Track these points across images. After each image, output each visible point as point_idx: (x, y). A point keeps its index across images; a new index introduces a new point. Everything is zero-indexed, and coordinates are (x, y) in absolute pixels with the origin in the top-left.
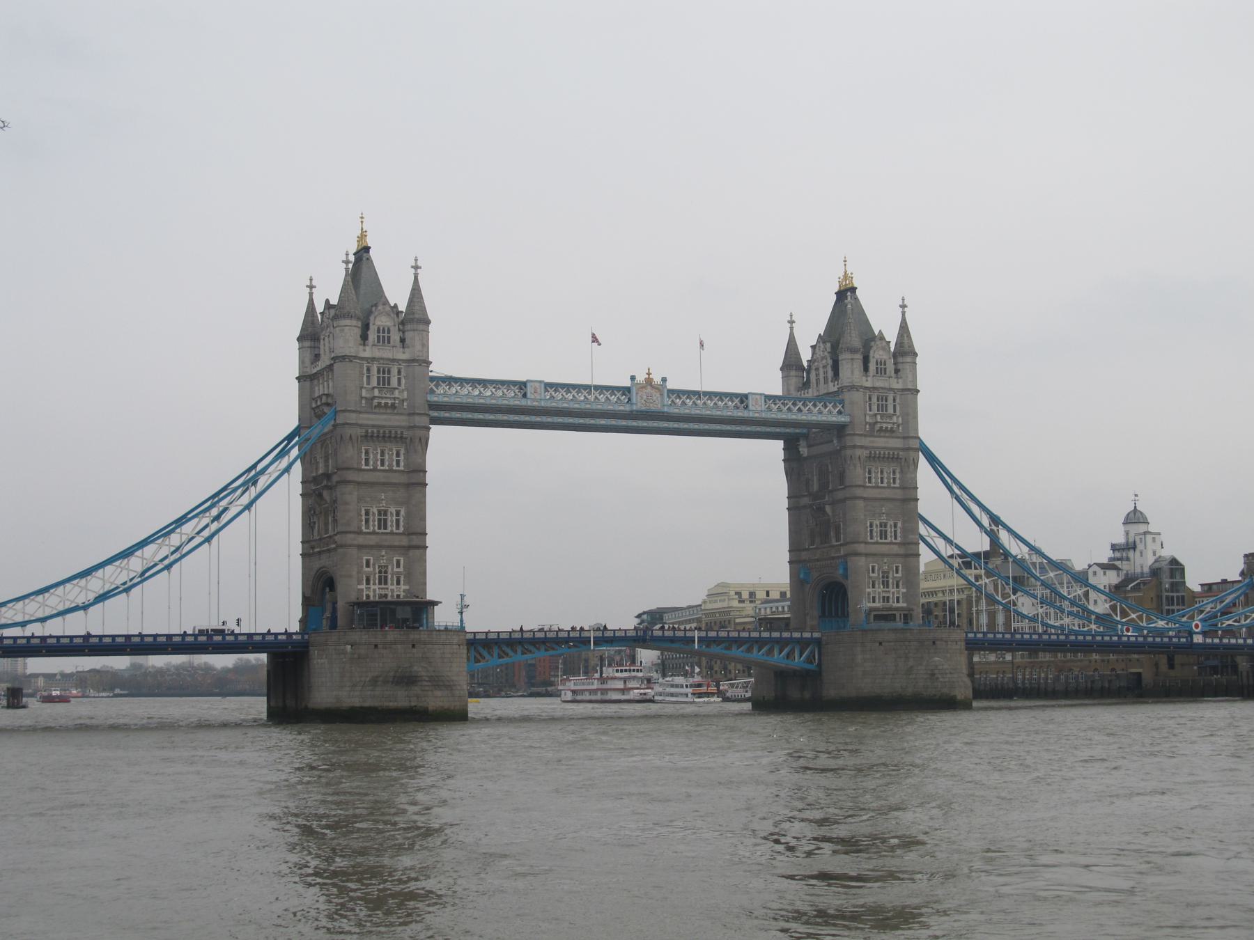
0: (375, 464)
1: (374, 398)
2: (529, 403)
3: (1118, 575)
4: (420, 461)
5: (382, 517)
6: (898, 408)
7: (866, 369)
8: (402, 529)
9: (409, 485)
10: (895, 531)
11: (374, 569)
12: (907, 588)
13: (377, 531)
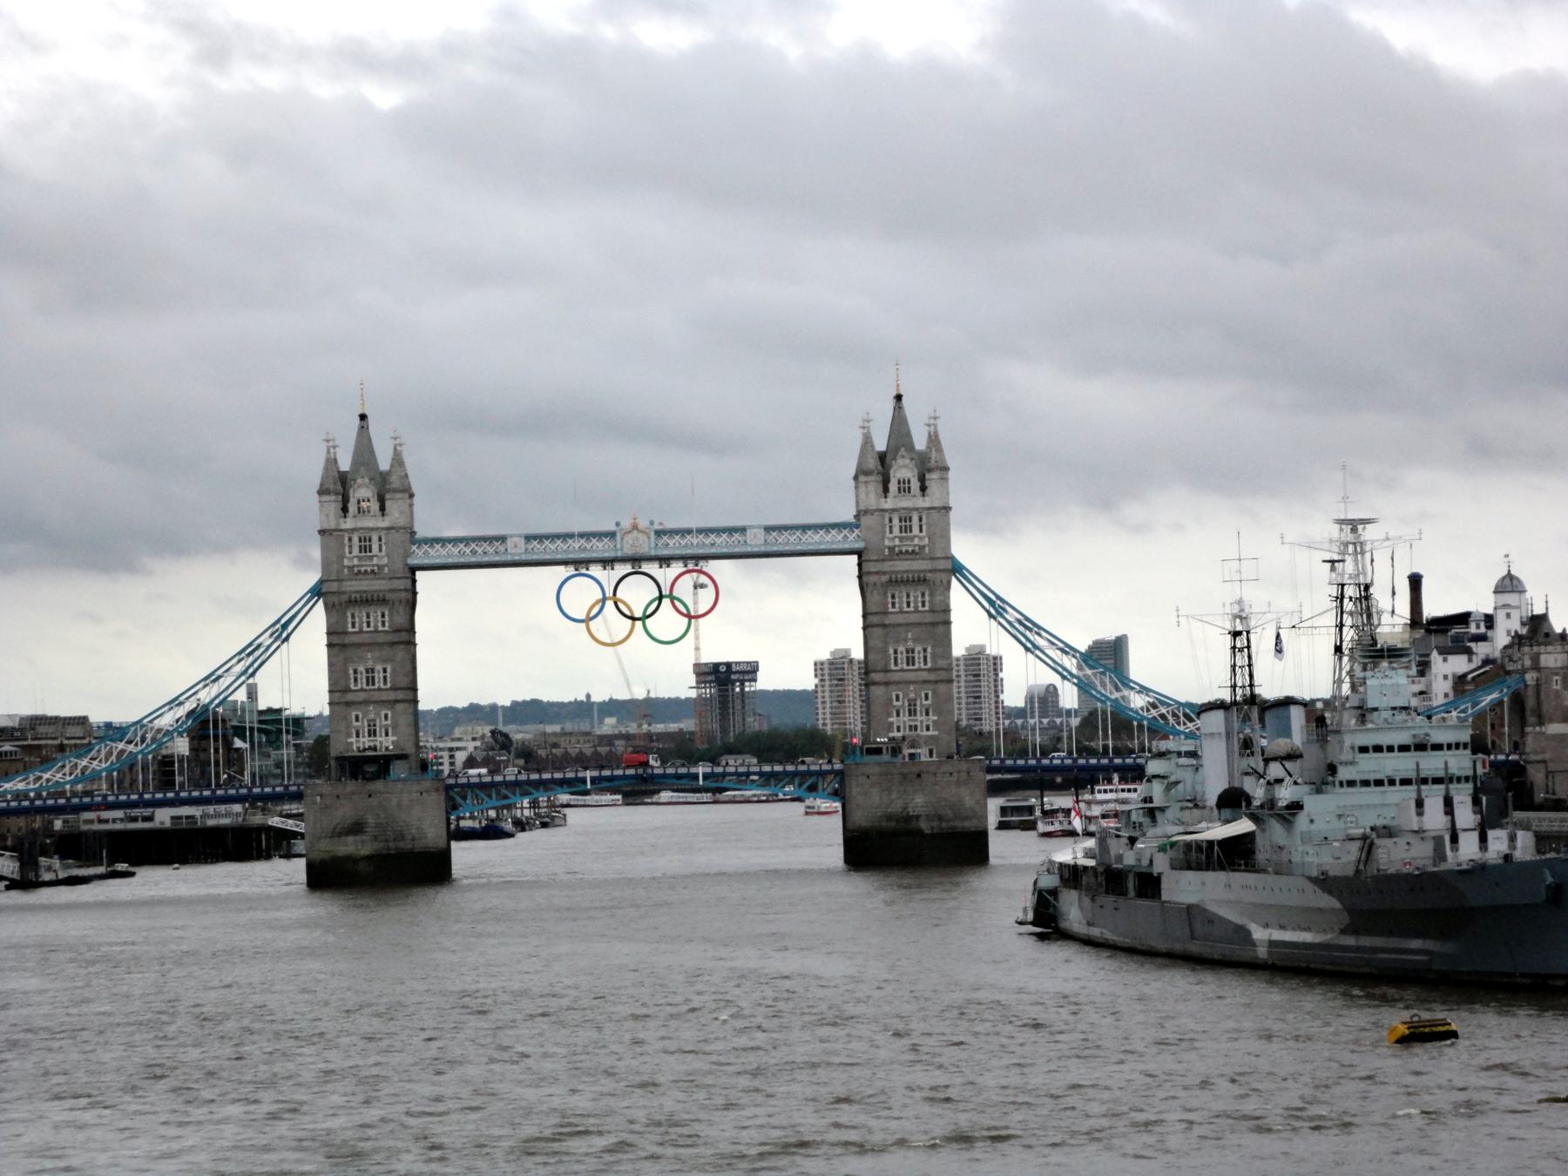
0: (361, 627)
1: (354, 566)
2: (509, 558)
3: (1470, 660)
4: (402, 621)
5: (370, 675)
6: (924, 528)
7: (886, 490)
8: (389, 685)
9: (393, 644)
10: (925, 658)
11: (363, 722)
12: (938, 716)
13: (365, 686)
